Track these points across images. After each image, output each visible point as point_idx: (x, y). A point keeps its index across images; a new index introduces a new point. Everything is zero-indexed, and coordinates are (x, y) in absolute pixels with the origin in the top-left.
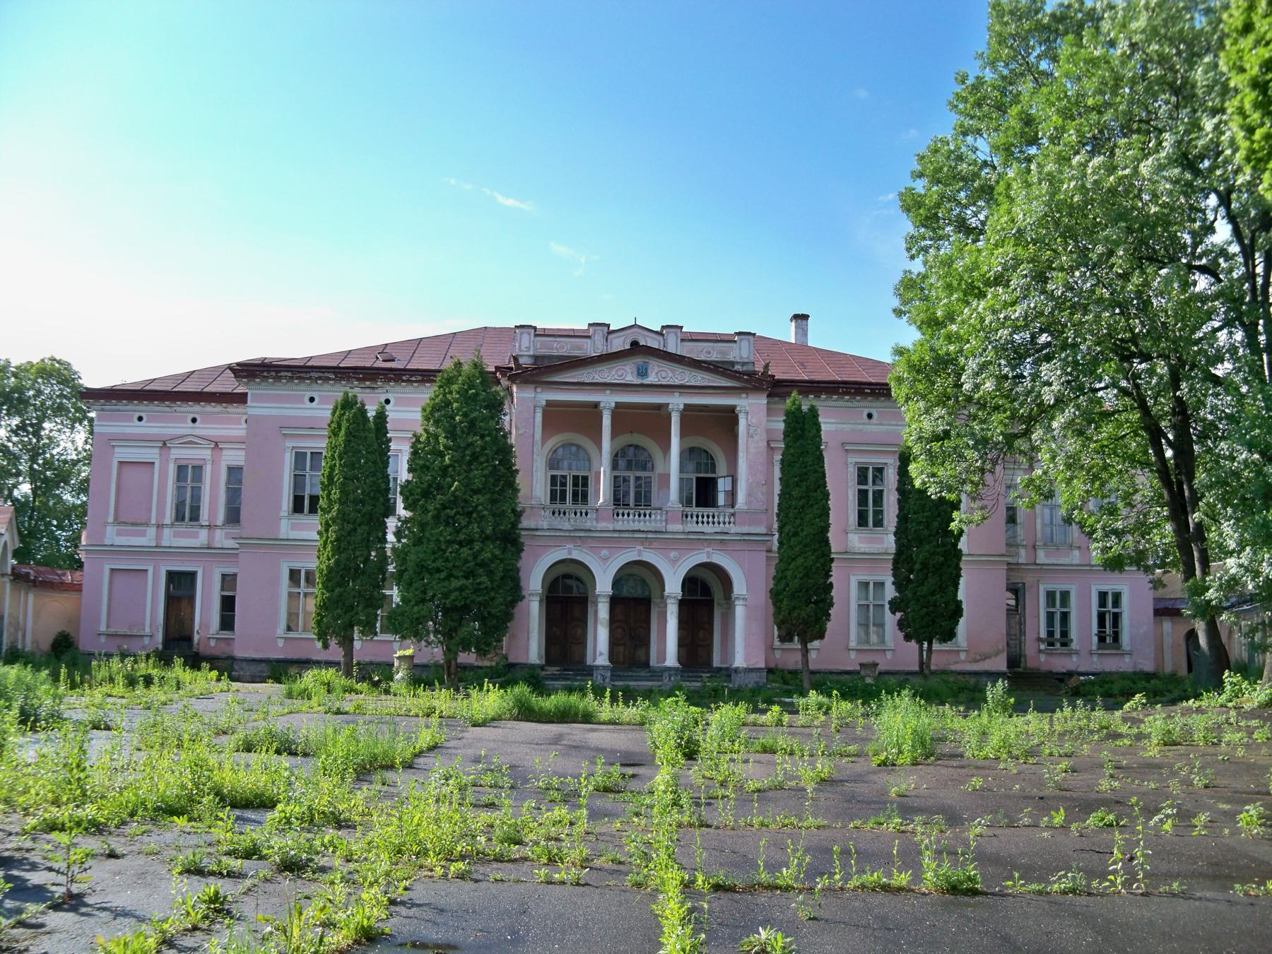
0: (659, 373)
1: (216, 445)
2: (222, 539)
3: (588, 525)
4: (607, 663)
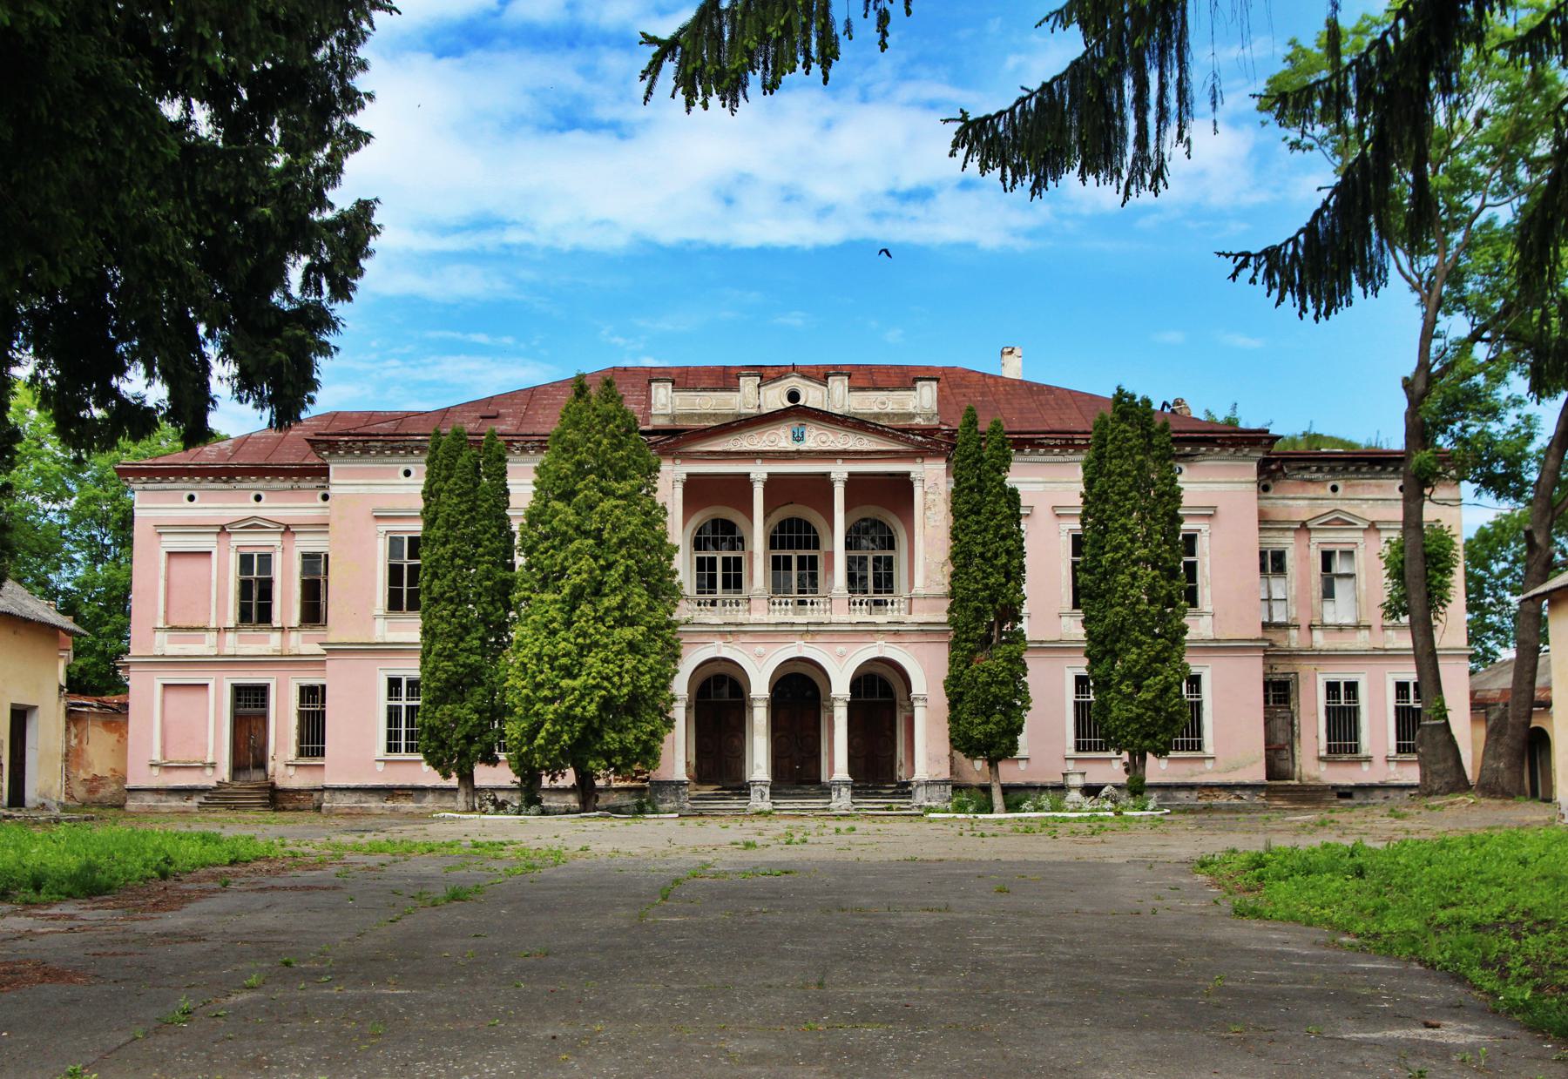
0: (817, 438)
1: (287, 530)
2: (304, 643)
3: (741, 617)
4: (847, 777)
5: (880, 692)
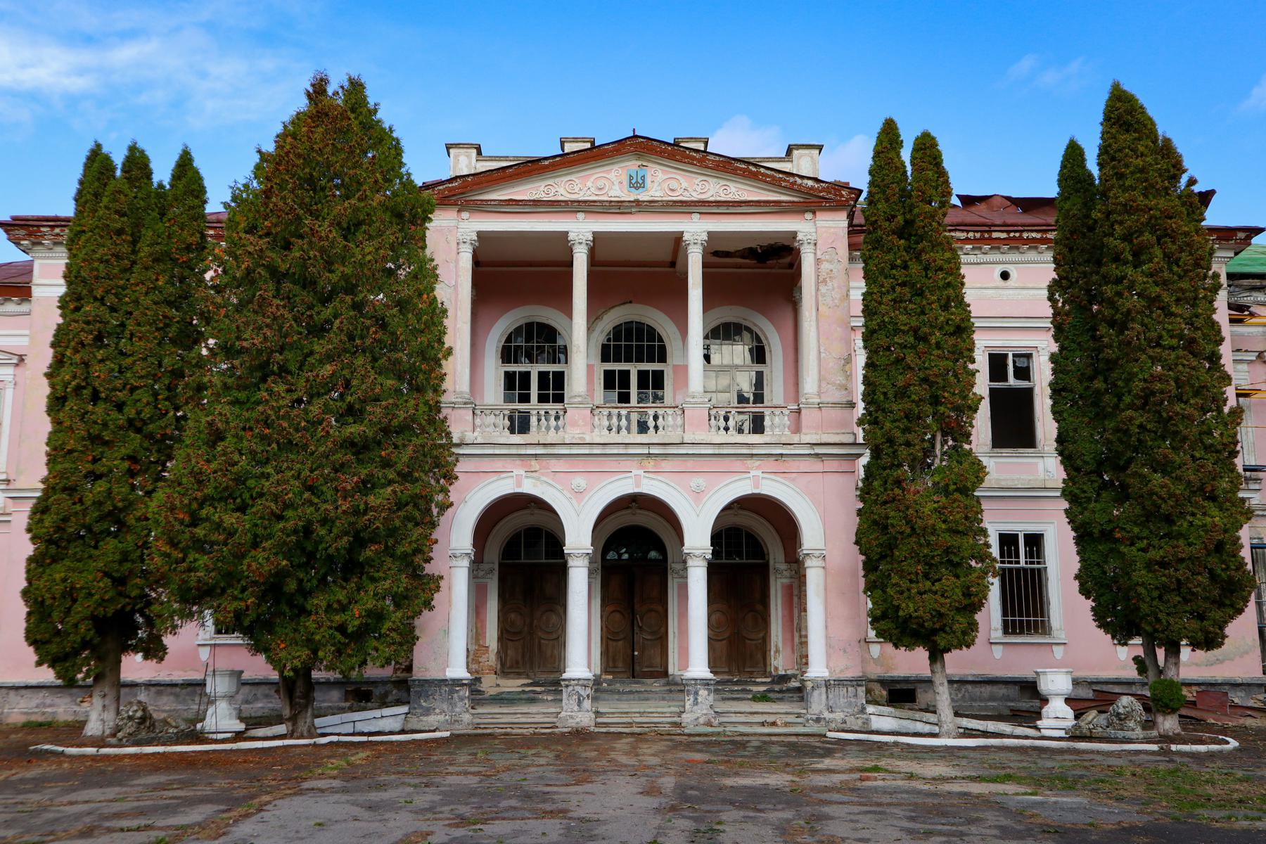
0: (664, 182)
5: (754, 548)
